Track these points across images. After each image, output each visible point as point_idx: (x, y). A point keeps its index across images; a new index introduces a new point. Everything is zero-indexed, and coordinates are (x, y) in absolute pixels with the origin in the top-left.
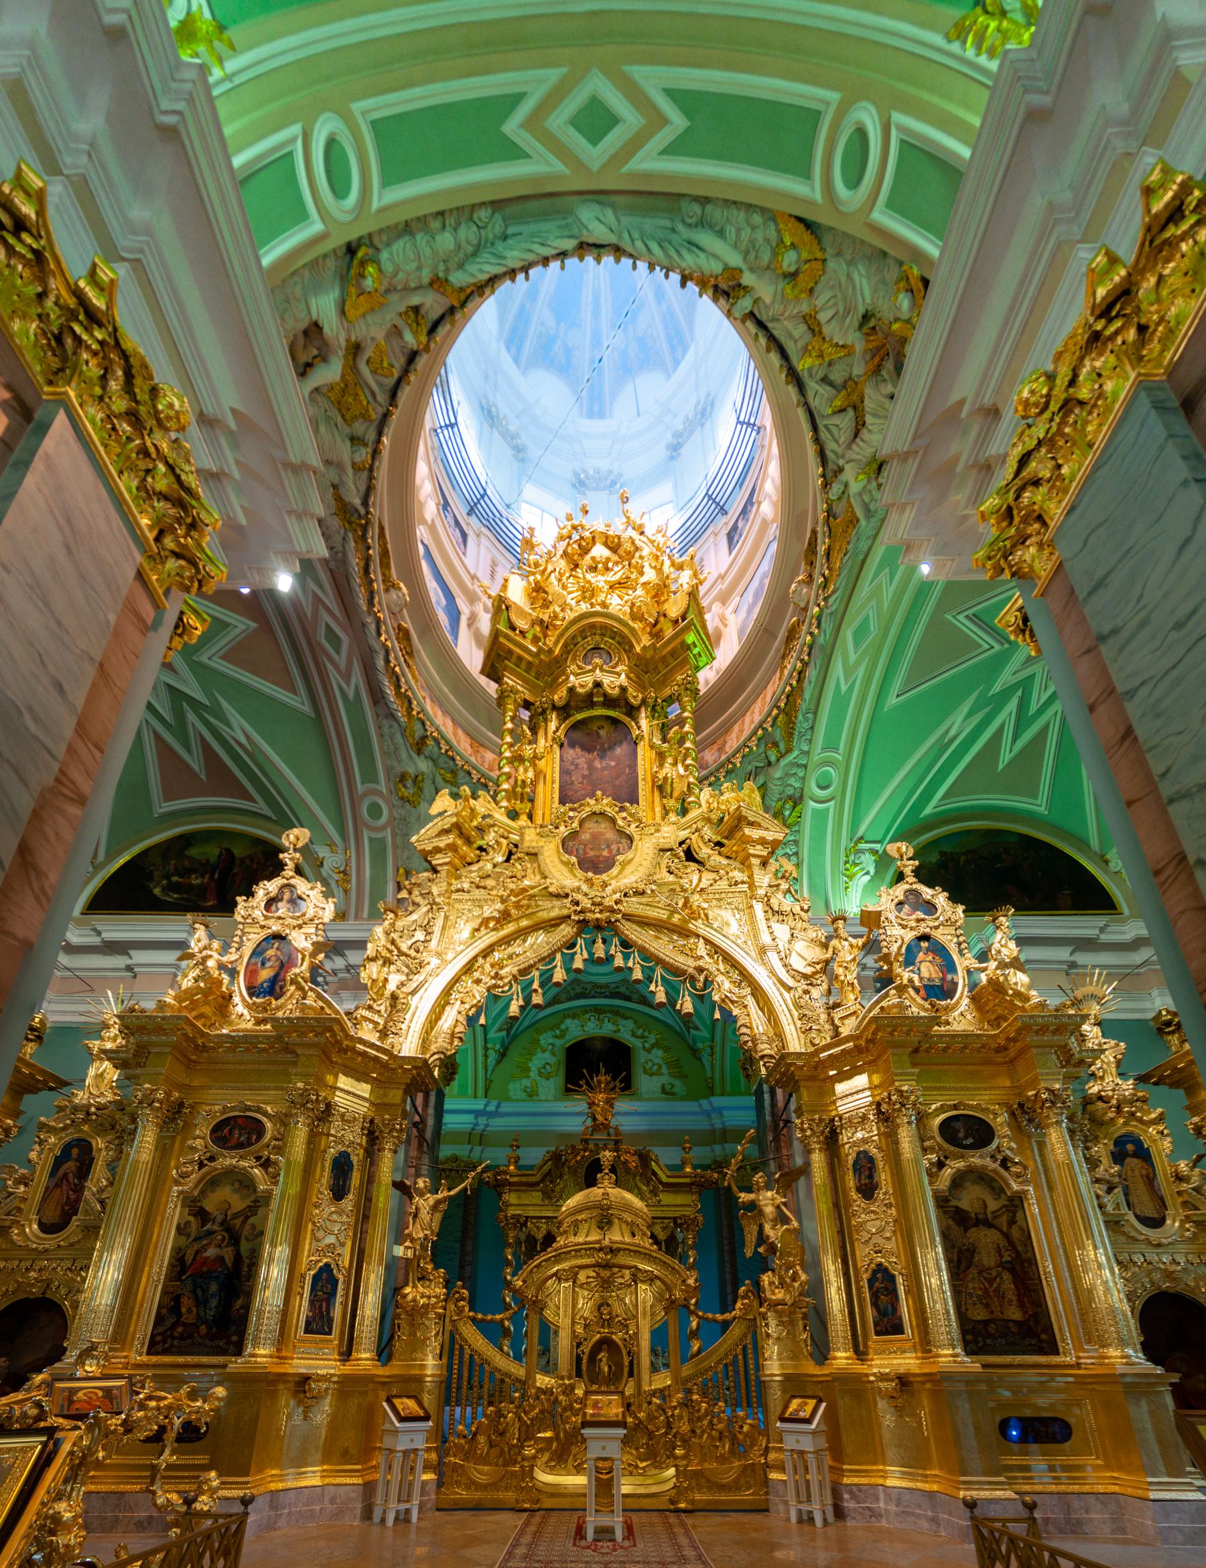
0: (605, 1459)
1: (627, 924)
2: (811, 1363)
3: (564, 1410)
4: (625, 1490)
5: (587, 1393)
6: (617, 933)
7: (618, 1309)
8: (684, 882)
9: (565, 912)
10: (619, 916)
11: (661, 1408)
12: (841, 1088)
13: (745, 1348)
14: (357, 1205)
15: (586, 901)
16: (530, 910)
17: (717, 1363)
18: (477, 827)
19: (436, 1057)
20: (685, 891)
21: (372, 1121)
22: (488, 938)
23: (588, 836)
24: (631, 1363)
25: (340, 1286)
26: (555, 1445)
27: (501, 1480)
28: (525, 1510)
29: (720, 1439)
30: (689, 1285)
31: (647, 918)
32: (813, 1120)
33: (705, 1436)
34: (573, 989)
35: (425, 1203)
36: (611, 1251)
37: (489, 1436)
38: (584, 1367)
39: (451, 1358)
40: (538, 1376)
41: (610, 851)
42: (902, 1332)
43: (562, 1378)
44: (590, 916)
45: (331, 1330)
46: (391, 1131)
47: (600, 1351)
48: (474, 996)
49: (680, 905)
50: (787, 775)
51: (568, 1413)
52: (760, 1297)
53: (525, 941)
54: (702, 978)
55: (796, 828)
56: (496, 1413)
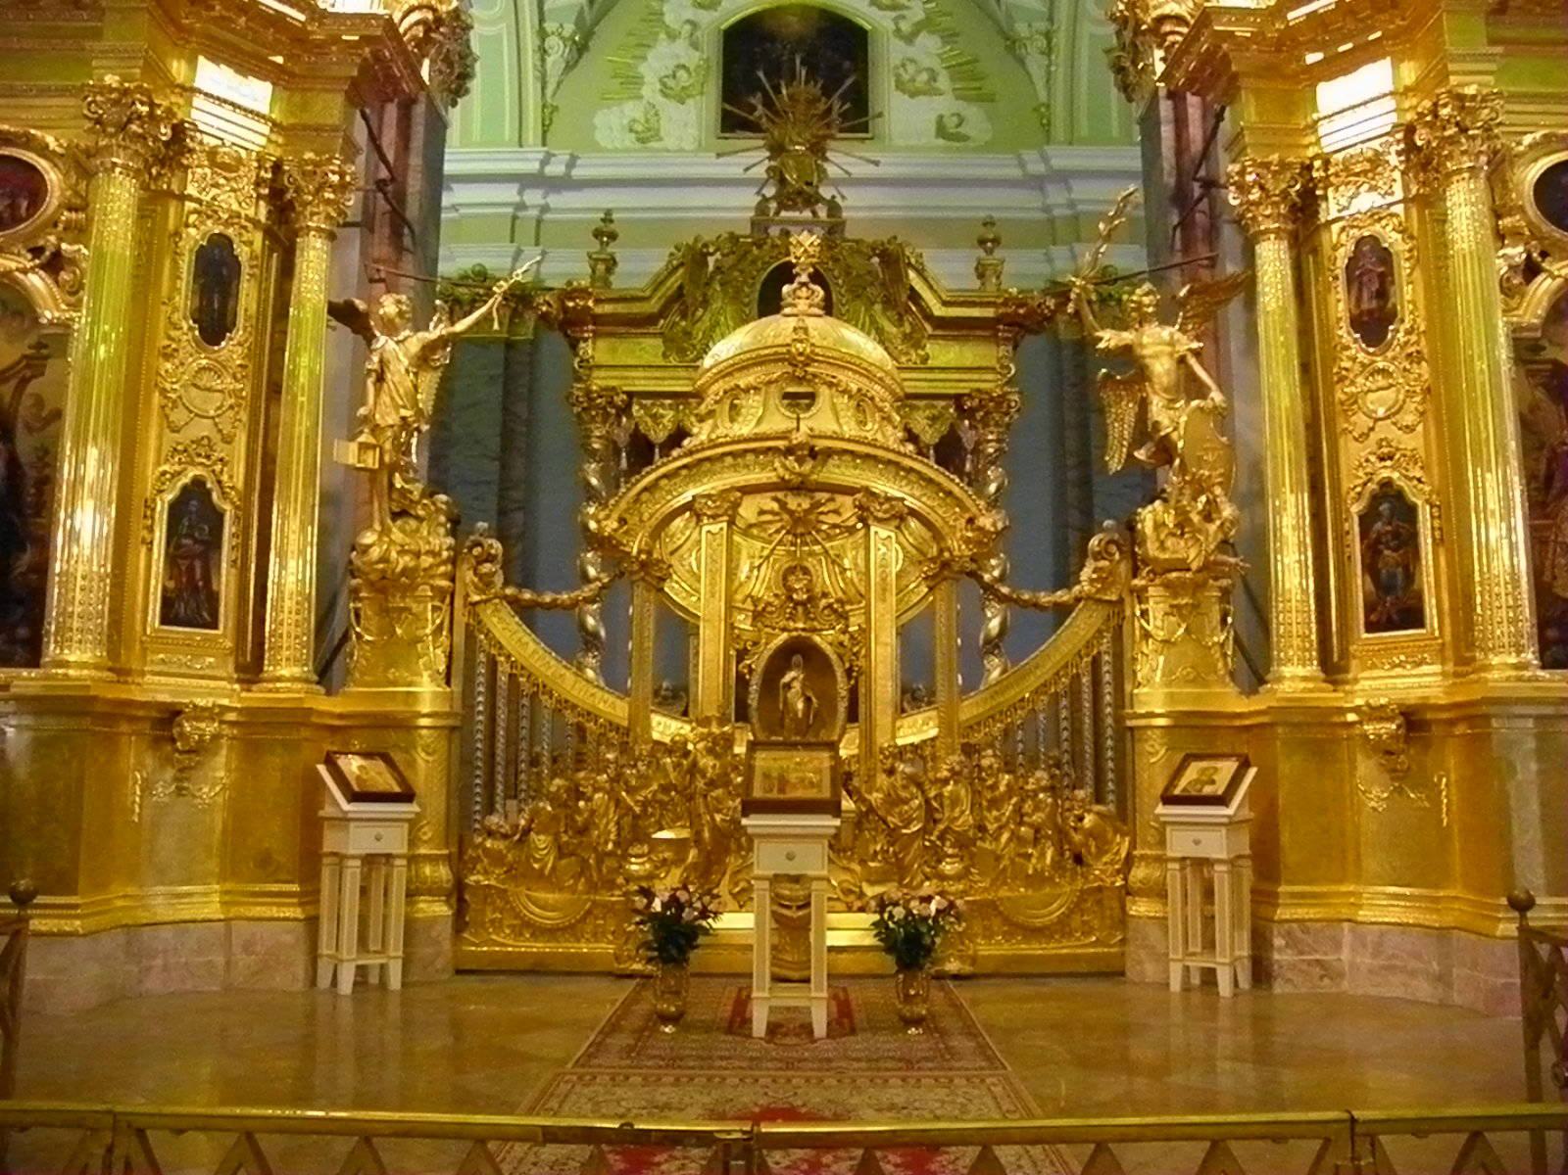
0: (796, 879)
2: (1232, 689)
3: (712, 784)
4: (834, 939)
5: (753, 746)
7: (825, 577)
12: (1330, 94)
13: (1096, 663)
14: (253, 353)
19: (415, 16)
21: (277, 168)
25: (228, 529)
26: (692, 854)
27: (583, 919)
28: (631, 976)
29: (1036, 841)
30: (981, 529)
32: (1266, 165)
37: (557, 837)
38: (753, 699)
39: (469, 680)
40: (656, 719)
42: (1419, 622)
45: (215, 614)
46: (319, 189)
51: (719, 792)
52: (1134, 554)
56: (568, 790)
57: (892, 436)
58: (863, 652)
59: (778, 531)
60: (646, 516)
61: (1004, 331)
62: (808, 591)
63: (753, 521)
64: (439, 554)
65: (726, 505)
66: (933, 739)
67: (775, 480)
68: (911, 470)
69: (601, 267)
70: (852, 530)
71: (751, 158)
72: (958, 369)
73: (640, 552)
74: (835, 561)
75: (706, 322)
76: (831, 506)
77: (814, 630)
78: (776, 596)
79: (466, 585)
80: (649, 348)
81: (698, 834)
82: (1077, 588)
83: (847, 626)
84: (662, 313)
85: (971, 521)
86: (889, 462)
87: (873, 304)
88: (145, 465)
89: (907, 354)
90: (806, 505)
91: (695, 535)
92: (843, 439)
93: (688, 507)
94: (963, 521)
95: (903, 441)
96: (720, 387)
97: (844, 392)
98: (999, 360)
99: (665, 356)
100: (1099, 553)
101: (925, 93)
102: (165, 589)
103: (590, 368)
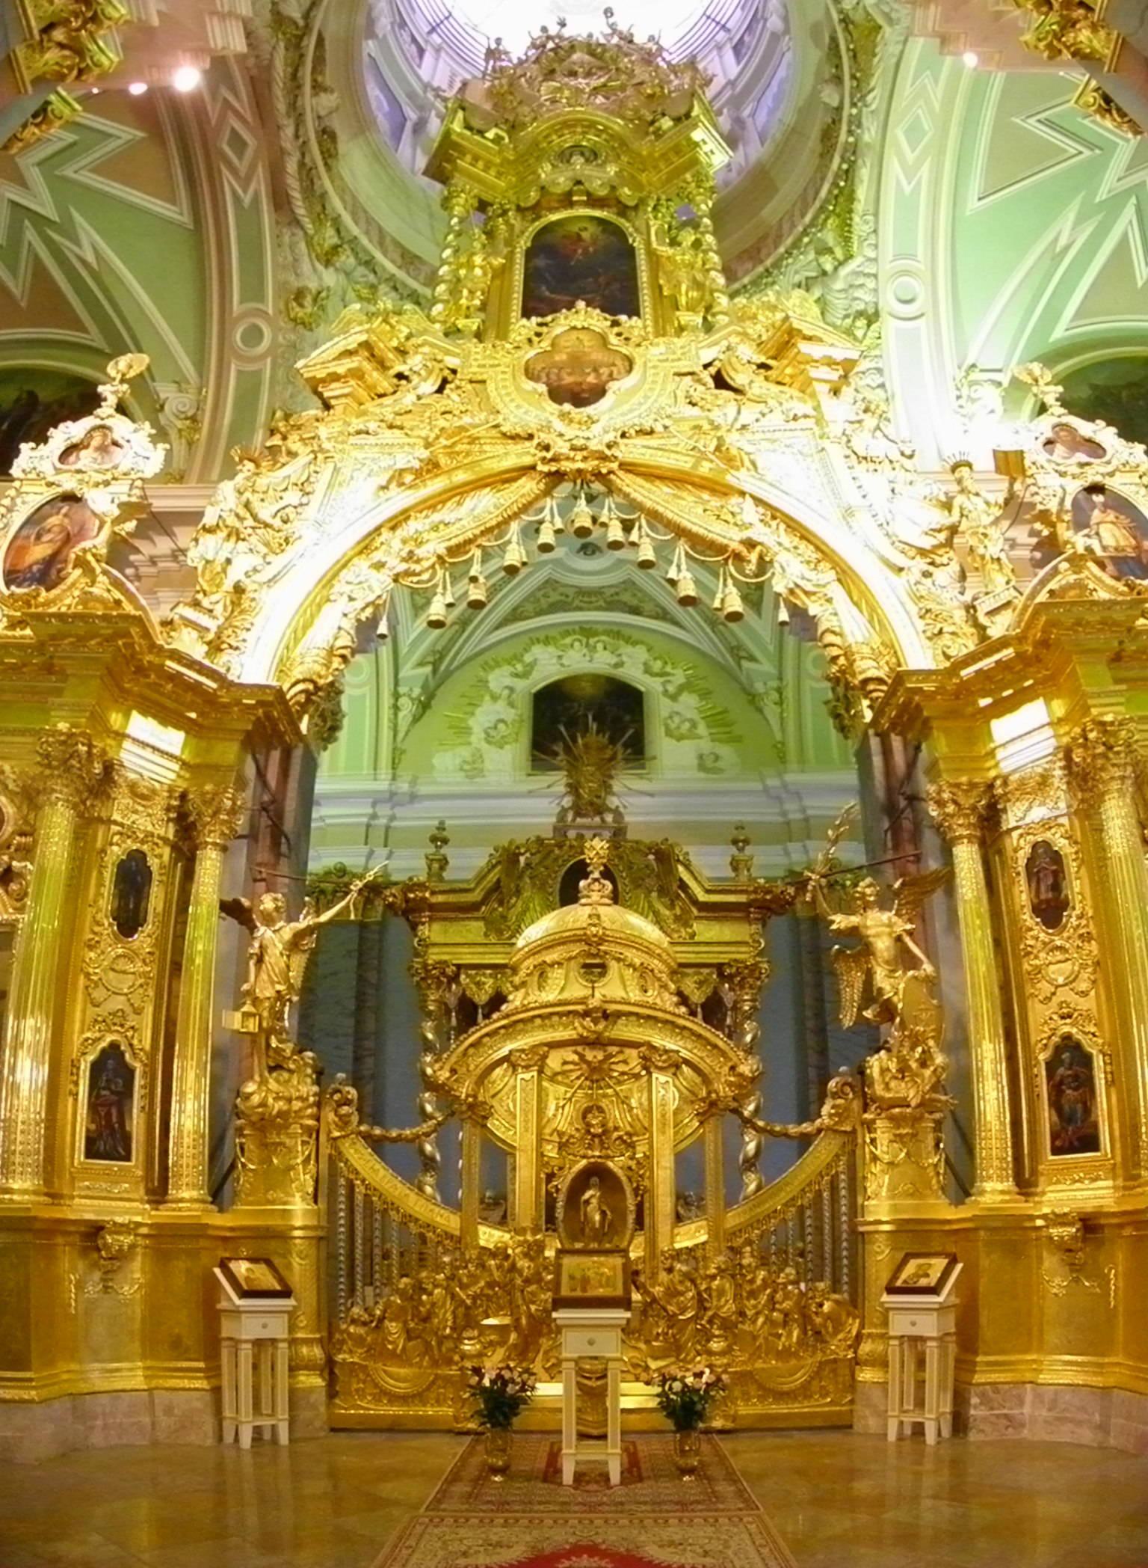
1: (628, 478)
6: (611, 490)
7: (617, 1116)
8: (716, 415)
9: (527, 460)
10: (615, 466)
11: (689, 1277)
15: (560, 442)
16: (470, 459)
17: (786, 1205)
18: (397, 349)
20: (717, 428)
22: (400, 499)
23: (564, 357)
24: (640, 1207)
30: (741, 1075)
31: (657, 467)
33: (761, 1320)
34: (545, 596)
35: (274, 937)
36: (606, 1016)
41: (598, 375)
43: (521, 1231)
44: (566, 466)
47: (586, 1187)
48: (370, 588)
49: (712, 448)
50: (851, 286)
53: (459, 504)
54: (754, 557)
55: (877, 352)
57: (669, 1001)
59: (578, 1078)
60: (472, 1067)
62: (603, 1126)
63: (558, 1069)
64: (307, 1099)
65: (537, 1058)
67: (575, 1037)
68: (684, 1028)
70: (637, 1076)
71: (557, 782)
72: (719, 943)
73: (468, 1096)
74: (624, 1101)
76: (620, 1058)
78: (577, 1130)
79: (328, 1123)
82: (819, 1121)
85: (733, 1068)
86: (666, 1022)
87: (650, 892)
88: (72, 1033)
89: (678, 931)
90: (600, 1056)
92: (629, 1004)
93: (505, 1059)
94: (726, 1069)
95: (677, 1005)
96: (530, 962)
97: (630, 965)
98: (751, 935)
100: (836, 1093)
101: (687, 738)
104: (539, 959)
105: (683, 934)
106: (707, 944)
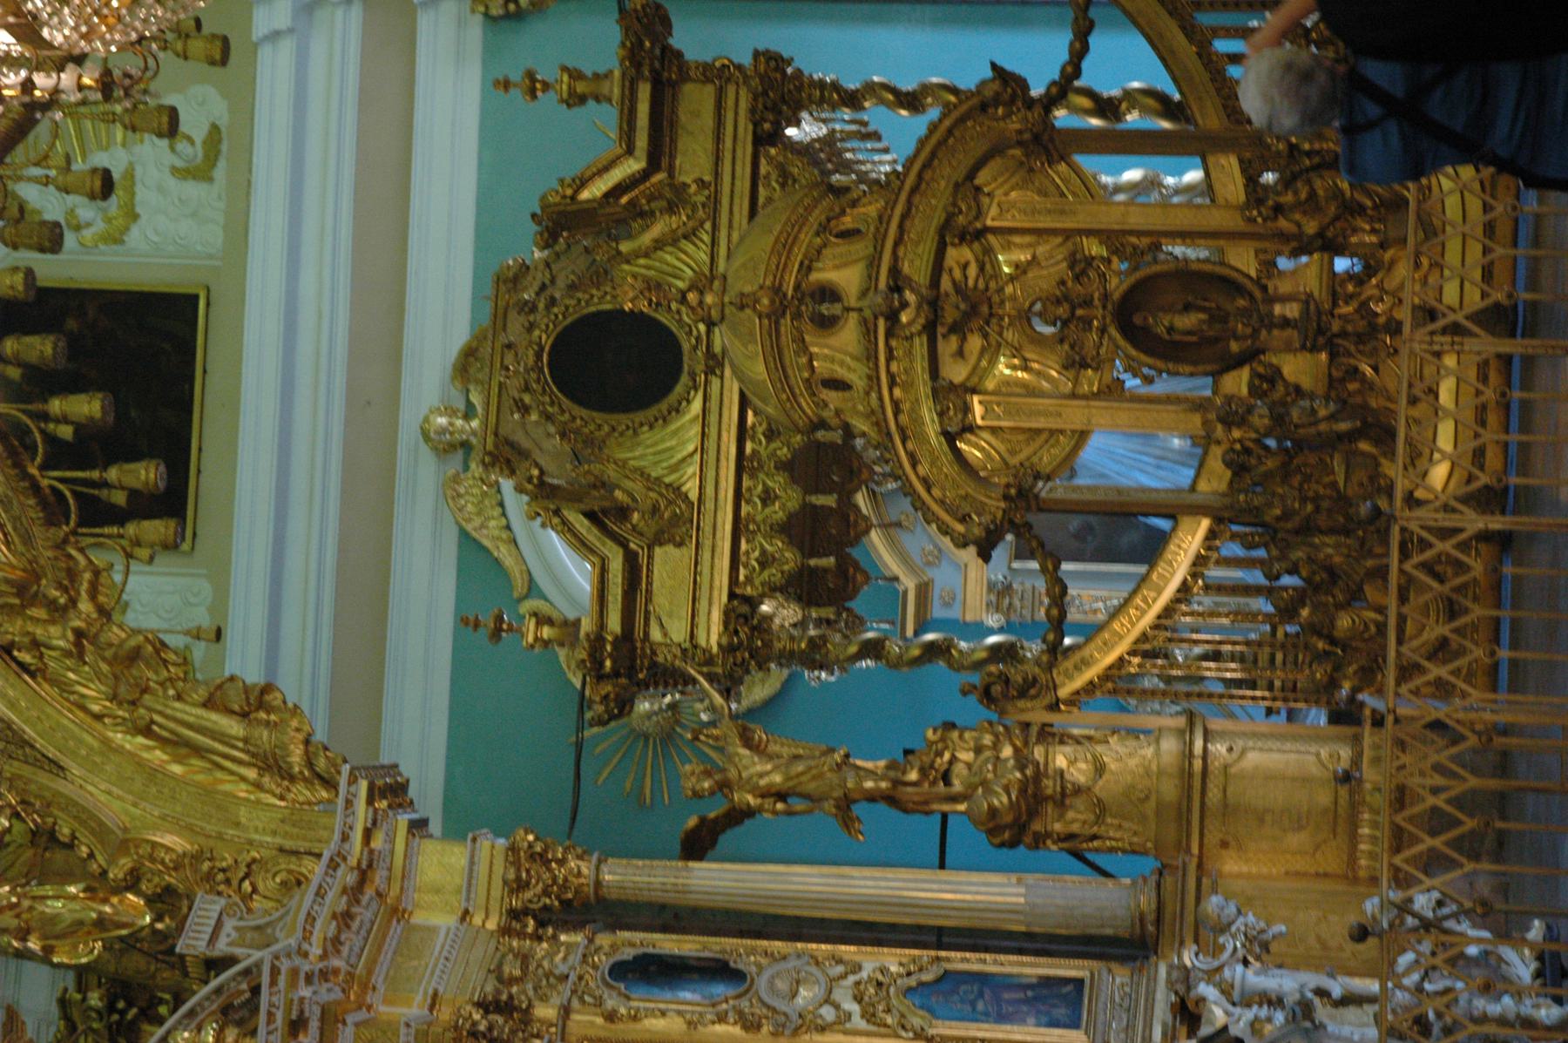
36: (896, 288)
58: (1134, 240)
61: (670, 71)
66: (1241, 161)
67: (925, 338)
69: (546, 632)
70: (989, 251)
72: (718, 138)
75: (637, 487)
77: (1106, 297)
80: (668, 565)
81: (1340, 437)
83: (1102, 258)
84: (623, 544)
86: (909, 202)
87: (619, 253)
91: (986, 435)
93: (950, 438)
99: (679, 545)
102: (1038, 1025)
103: (695, 647)
104: (800, 388)
105: (700, 199)
106: (718, 159)
